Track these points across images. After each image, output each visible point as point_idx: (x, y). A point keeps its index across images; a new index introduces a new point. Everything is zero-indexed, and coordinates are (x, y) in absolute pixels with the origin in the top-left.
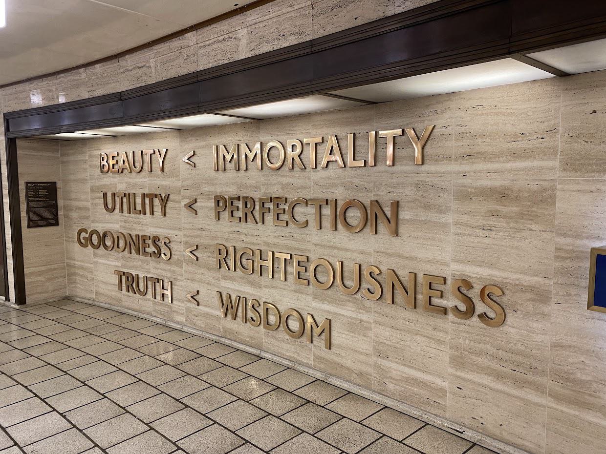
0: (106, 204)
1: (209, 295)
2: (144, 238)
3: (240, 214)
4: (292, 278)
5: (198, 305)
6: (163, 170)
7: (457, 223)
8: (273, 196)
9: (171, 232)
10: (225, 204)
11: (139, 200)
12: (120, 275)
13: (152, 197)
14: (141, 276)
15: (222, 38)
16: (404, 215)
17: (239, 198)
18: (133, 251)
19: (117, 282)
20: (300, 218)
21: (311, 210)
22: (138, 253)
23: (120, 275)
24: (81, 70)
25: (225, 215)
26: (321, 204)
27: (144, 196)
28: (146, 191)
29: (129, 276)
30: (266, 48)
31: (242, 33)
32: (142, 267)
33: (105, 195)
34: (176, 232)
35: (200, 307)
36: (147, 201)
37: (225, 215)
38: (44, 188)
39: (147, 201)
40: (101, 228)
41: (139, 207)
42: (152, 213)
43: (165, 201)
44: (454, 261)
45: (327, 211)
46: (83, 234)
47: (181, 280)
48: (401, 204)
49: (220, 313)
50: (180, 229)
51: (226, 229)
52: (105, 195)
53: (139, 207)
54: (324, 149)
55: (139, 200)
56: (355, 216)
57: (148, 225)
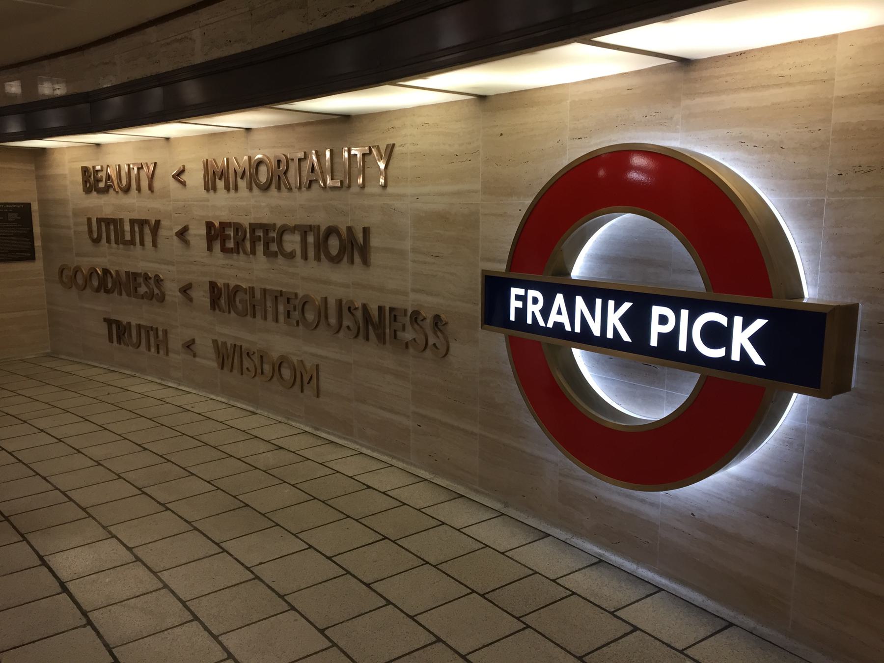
0: (90, 231)
1: (204, 345)
2: (135, 275)
3: (231, 244)
4: (281, 318)
5: (195, 356)
6: (151, 188)
7: (414, 250)
8: (265, 221)
9: (163, 267)
10: (217, 233)
11: (127, 228)
12: (109, 322)
13: (142, 223)
14: (134, 323)
15: (179, 37)
16: (375, 242)
17: (229, 224)
18: (124, 293)
19: (105, 331)
20: (288, 248)
21: (297, 238)
22: (129, 295)
23: (109, 322)
24: (45, 62)
25: (217, 246)
26: (304, 230)
27: (132, 222)
28: (135, 216)
29: (118, 323)
30: (217, 54)
31: (196, 34)
32: (134, 313)
33: (89, 220)
34: (171, 268)
35: (197, 359)
36: (137, 229)
37: (217, 246)
38: (15, 210)
39: (137, 229)
40: (85, 263)
41: (128, 237)
42: (142, 243)
43: (156, 227)
44: (413, 290)
45: (311, 239)
46: (65, 272)
48: (373, 230)
49: (214, 365)
50: (172, 264)
52: (89, 220)
53: (128, 237)
54: (306, 166)
55: (127, 228)
56: (334, 244)
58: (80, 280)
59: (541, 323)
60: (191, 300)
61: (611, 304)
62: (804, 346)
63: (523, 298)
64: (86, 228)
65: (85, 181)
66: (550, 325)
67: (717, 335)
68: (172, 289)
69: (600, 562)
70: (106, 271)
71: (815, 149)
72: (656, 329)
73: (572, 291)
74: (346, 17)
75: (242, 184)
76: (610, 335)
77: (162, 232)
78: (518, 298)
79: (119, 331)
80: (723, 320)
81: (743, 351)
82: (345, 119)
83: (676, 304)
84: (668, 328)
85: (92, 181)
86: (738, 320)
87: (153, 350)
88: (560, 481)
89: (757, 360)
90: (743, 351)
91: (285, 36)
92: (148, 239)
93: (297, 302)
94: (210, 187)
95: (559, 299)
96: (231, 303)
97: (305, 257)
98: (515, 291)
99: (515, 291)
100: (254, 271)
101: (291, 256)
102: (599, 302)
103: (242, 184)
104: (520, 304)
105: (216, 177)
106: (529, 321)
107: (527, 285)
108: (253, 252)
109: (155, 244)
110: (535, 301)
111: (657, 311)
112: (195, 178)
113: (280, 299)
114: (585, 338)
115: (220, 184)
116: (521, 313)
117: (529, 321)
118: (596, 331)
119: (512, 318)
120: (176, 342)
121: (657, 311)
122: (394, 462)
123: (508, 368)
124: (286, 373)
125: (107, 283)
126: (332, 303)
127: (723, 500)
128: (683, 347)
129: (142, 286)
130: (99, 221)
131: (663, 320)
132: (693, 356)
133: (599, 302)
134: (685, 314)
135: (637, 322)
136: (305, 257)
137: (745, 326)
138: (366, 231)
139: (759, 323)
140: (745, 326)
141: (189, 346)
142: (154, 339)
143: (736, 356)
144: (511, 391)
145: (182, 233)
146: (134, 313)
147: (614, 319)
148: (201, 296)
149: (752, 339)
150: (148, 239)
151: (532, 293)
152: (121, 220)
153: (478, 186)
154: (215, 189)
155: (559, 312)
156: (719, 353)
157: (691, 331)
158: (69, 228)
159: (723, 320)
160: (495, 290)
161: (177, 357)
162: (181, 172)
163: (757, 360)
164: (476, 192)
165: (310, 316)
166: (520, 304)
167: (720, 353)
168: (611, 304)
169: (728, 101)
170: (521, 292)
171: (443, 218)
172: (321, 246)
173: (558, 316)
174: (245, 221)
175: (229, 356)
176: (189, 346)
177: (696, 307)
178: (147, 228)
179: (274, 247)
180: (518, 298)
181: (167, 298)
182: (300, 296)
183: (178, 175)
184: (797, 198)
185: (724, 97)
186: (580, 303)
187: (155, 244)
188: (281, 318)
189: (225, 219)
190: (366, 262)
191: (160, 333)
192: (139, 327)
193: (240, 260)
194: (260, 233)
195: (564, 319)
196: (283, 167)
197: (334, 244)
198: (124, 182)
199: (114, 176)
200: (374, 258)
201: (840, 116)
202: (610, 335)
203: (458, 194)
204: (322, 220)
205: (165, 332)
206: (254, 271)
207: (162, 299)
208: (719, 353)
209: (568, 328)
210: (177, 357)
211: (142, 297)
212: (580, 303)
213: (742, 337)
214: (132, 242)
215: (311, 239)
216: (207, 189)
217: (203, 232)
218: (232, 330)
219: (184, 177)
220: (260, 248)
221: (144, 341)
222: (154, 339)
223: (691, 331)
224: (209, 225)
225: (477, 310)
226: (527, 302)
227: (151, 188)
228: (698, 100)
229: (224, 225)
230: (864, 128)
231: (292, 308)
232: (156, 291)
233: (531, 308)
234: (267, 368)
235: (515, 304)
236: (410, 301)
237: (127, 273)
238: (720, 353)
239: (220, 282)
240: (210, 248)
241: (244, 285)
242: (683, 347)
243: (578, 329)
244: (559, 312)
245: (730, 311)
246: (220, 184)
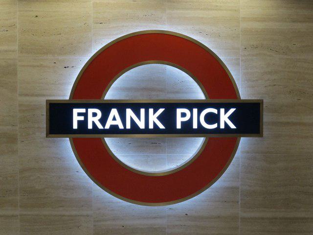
59: (100, 126)
61: (151, 111)
62: (249, 117)
63: (85, 115)
66: (107, 127)
71: (234, 37)
72: (179, 120)
76: (151, 126)
78: (79, 114)
80: (215, 111)
83: (190, 105)
86: (222, 110)
88: (95, 226)
89: (232, 126)
95: (114, 112)
98: (76, 111)
99: (76, 111)
102: (143, 111)
104: (82, 118)
106: (90, 126)
107: (87, 106)
110: (95, 115)
111: (179, 111)
117: (90, 126)
118: (141, 125)
119: (75, 126)
121: (179, 111)
127: (202, 201)
128: (195, 126)
131: (183, 115)
132: (201, 131)
133: (143, 111)
134: (195, 111)
135: (168, 118)
139: (232, 110)
140: (226, 112)
143: (222, 126)
149: (230, 118)
151: (91, 111)
153: (16, 47)
155: (114, 119)
157: (198, 119)
159: (215, 111)
163: (232, 126)
164: (13, 51)
167: (215, 126)
168: (151, 111)
170: (83, 110)
177: (201, 106)
180: (79, 114)
184: (228, 58)
186: (129, 113)
195: (119, 123)
201: (244, 25)
209: (121, 127)
212: (129, 113)
213: (225, 118)
223: (198, 119)
230: (253, 30)
233: (91, 119)
235: (76, 119)
238: (215, 126)
242: (195, 126)
243: (128, 126)
244: (114, 119)
245: (218, 106)
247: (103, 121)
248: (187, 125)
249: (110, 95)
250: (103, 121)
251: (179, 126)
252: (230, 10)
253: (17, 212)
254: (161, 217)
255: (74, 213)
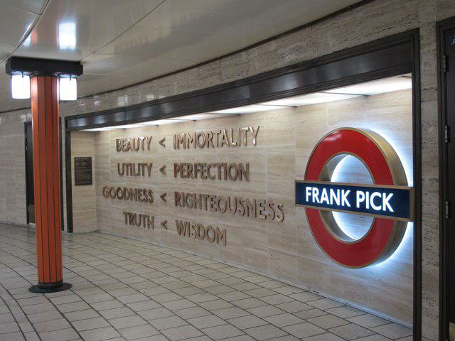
0: (119, 170)
3: (185, 174)
6: (149, 149)
7: (269, 173)
8: (201, 162)
9: (153, 186)
10: (178, 169)
11: (136, 167)
12: (126, 214)
13: (144, 165)
14: (138, 214)
16: (251, 170)
19: (124, 219)
20: (212, 174)
23: (126, 214)
24: (106, 94)
25: (179, 174)
26: (220, 166)
27: (139, 165)
29: (130, 215)
31: (175, 83)
32: (137, 208)
34: (156, 186)
36: (141, 168)
37: (179, 174)
38: (85, 161)
39: (141, 168)
40: (116, 186)
41: (137, 172)
42: (143, 175)
45: (222, 170)
47: (158, 215)
49: (176, 233)
51: (181, 182)
53: (137, 172)
54: (221, 136)
55: (136, 167)
56: (233, 172)
57: (142, 183)
58: (113, 194)
59: (318, 201)
60: (166, 201)
61: (343, 191)
62: (406, 203)
64: (117, 169)
65: (117, 147)
66: (321, 202)
67: (378, 201)
68: (156, 196)
69: (345, 306)
70: (125, 189)
72: (359, 201)
73: (329, 187)
74: (236, 79)
75: (192, 145)
77: (153, 169)
78: (309, 191)
79: (131, 218)
81: (387, 208)
82: (239, 115)
83: (364, 189)
84: (362, 200)
85: (120, 147)
86: (384, 194)
87: (146, 227)
89: (391, 210)
90: (387, 208)
91: (212, 85)
92: (146, 172)
93: (216, 200)
94: (176, 147)
95: (324, 191)
96: (185, 201)
97: (220, 178)
98: (308, 188)
99: (308, 188)
100: (196, 186)
101: (214, 178)
102: (338, 191)
103: (192, 145)
104: (310, 194)
105: (180, 142)
108: (196, 177)
109: (149, 175)
111: (359, 193)
112: (170, 143)
113: (208, 199)
114: (335, 207)
115: (181, 145)
116: (310, 197)
117: (314, 201)
118: (338, 204)
119: (307, 200)
120: (158, 223)
121: (359, 193)
122: (261, 273)
123: (307, 224)
124: (211, 235)
125: (123, 194)
126: (232, 199)
129: (144, 196)
130: (124, 165)
131: (361, 196)
132: (371, 211)
133: (338, 191)
134: (367, 193)
135: (352, 198)
136: (220, 178)
137: (387, 196)
138: (248, 165)
141: (164, 224)
142: (148, 221)
143: (384, 209)
144: (309, 235)
145: (162, 170)
146: (137, 208)
147: (343, 198)
148: (171, 199)
150: (146, 172)
152: (134, 164)
153: (295, 145)
154: (179, 148)
156: (378, 208)
158: (109, 169)
160: (300, 187)
161: (158, 229)
162: (164, 140)
163: (391, 210)
165: (222, 206)
166: (310, 194)
169: (381, 111)
171: (281, 159)
172: (227, 173)
173: (324, 198)
174: (193, 163)
175: (182, 228)
176: (164, 224)
177: (371, 190)
178: (146, 167)
179: (205, 174)
180: (309, 191)
181: (154, 201)
182: (217, 196)
183: (162, 142)
185: (379, 109)
187: (149, 175)
188: (209, 208)
189: (183, 162)
190: (247, 180)
191: (150, 219)
192: (140, 216)
193: (190, 181)
194: (199, 168)
196: (211, 136)
197: (233, 172)
198: (136, 146)
199: (132, 143)
200: (251, 177)
202: (343, 204)
203: (287, 147)
204: (228, 161)
205: (153, 218)
206: (196, 186)
207: (151, 201)
208: (378, 208)
209: (328, 203)
210: (158, 229)
211: (142, 201)
212: (332, 190)
213: (386, 200)
214: (139, 175)
215: (222, 170)
216: (175, 148)
217: (173, 168)
218: (186, 215)
219: (164, 143)
220: (199, 175)
221: (142, 223)
222: (148, 221)
224: (176, 165)
225: (293, 198)
226: (312, 193)
227: (149, 149)
228: (372, 110)
229: (182, 165)
231: (213, 203)
232: (149, 198)
234: (201, 233)
235: (308, 194)
236: (268, 196)
237: (136, 189)
239: (181, 192)
240: (175, 176)
241: (191, 193)
242: (367, 207)
245: (381, 191)
246: (181, 145)
247: (320, 197)
248: (363, 204)
249: (335, 178)
250: (320, 197)
251: (358, 206)
252: (406, 105)
253: (296, 254)
254: (366, 278)
255: (321, 262)
